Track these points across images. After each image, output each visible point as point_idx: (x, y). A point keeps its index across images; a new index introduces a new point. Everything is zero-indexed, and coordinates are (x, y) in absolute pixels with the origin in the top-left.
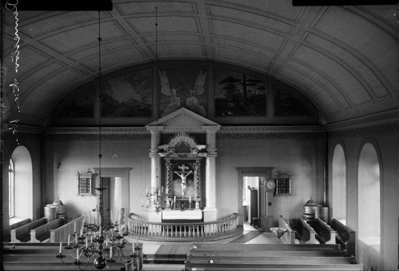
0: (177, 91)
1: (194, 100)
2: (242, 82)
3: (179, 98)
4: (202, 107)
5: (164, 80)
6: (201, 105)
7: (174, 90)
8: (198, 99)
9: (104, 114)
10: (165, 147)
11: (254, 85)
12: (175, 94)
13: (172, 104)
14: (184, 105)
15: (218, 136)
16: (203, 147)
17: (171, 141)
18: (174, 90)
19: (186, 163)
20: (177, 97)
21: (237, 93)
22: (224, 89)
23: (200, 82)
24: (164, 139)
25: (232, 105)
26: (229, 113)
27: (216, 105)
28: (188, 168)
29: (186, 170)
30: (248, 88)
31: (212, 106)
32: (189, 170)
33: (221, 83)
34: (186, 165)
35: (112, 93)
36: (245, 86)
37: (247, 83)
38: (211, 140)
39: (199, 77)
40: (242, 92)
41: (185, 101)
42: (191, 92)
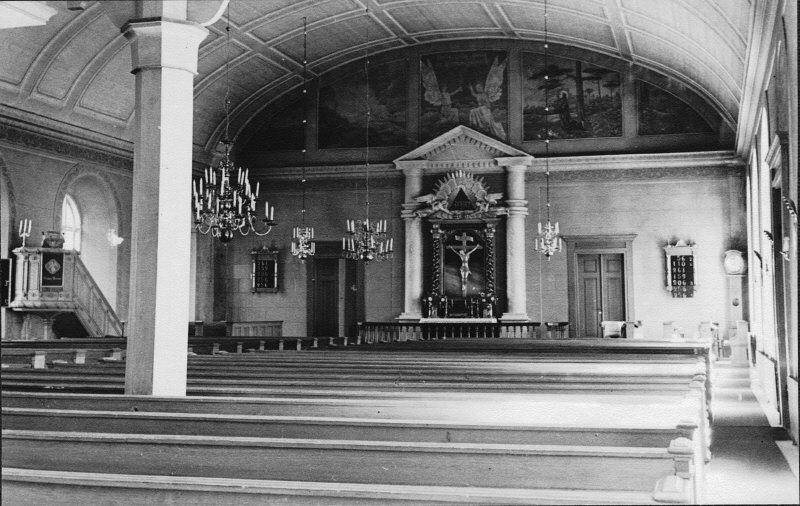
0: (452, 98)
1: (484, 111)
2: (574, 73)
4: (498, 125)
5: (431, 78)
6: (497, 120)
8: (492, 111)
10: (428, 198)
11: (598, 78)
12: (449, 102)
14: (465, 122)
15: (530, 177)
16: (499, 196)
17: (441, 188)
18: (447, 96)
19: (468, 228)
20: (453, 107)
21: (564, 95)
22: (541, 88)
23: (495, 80)
24: (431, 183)
25: (555, 118)
27: (525, 119)
28: (472, 239)
29: (469, 243)
30: (586, 85)
31: (517, 121)
32: (474, 244)
34: (469, 235)
36: (579, 81)
37: (584, 75)
38: (518, 187)
39: (493, 68)
40: (574, 92)
41: (467, 113)
42: (479, 97)
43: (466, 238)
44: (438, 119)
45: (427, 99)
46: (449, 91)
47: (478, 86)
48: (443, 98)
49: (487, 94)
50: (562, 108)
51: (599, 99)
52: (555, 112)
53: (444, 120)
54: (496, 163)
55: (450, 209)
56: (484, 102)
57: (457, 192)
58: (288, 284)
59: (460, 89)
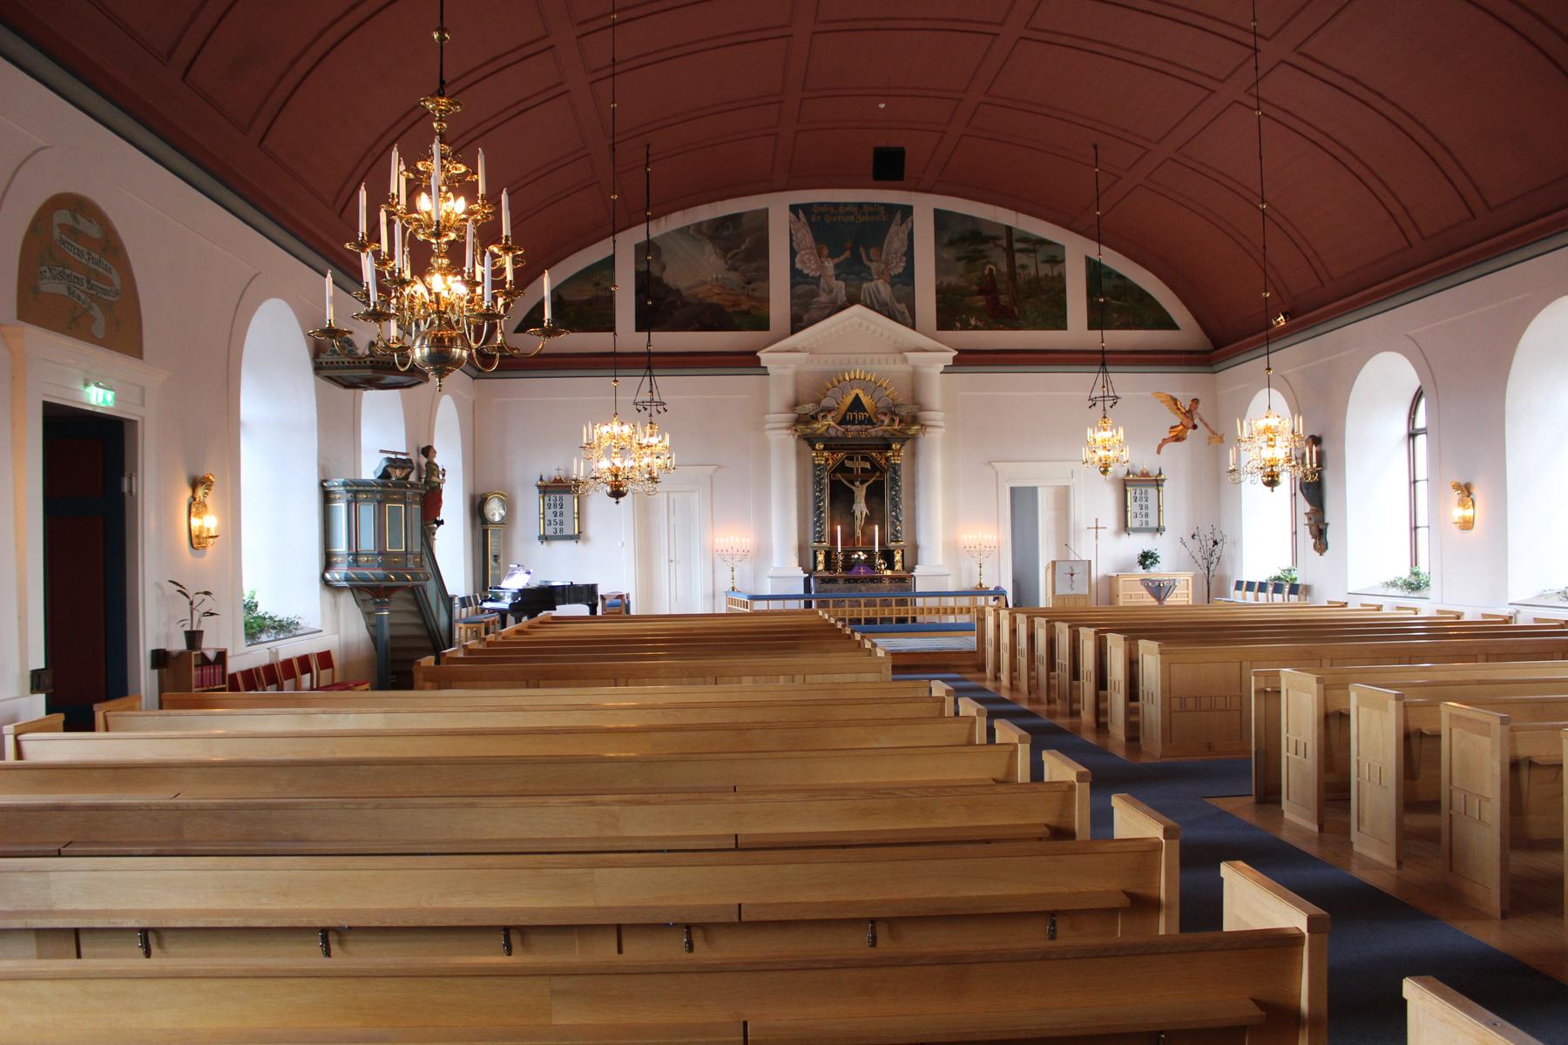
0: (837, 266)
2: (1004, 242)
3: (842, 284)
6: (899, 301)
7: (829, 265)
8: (892, 285)
9: (646, 321)
11: (1035, 251)
13: (824, 298)
14: (852, 301)
18: (829, 265)
22: (959, 259)
25: (980, 301)
26: (973, 322)
28: (868, 466)
30: (1020, 259)
33: (952, 243)
34: (864, 459)
35: (663, 269)
36: (1010, 253)
37: (1017, 246)
39: (893, 228)
40: (1004, 267)
41: (859, 288)
42: (874, 266)
43: (859, 465)
44: (816, 295)
45: (798, 266)
46: (832, 256)
47: (873, 251)
48: (821, 267)
49: (887, 263)
50: (988, 288)
51: (1037, 279)
52: (980, 293)
53: (824, 298)
54: (905, 360)
55: (839, 424)
56: (881, 274)
57: (849, 400)
58: (593, 527)
59: (847, 254)
